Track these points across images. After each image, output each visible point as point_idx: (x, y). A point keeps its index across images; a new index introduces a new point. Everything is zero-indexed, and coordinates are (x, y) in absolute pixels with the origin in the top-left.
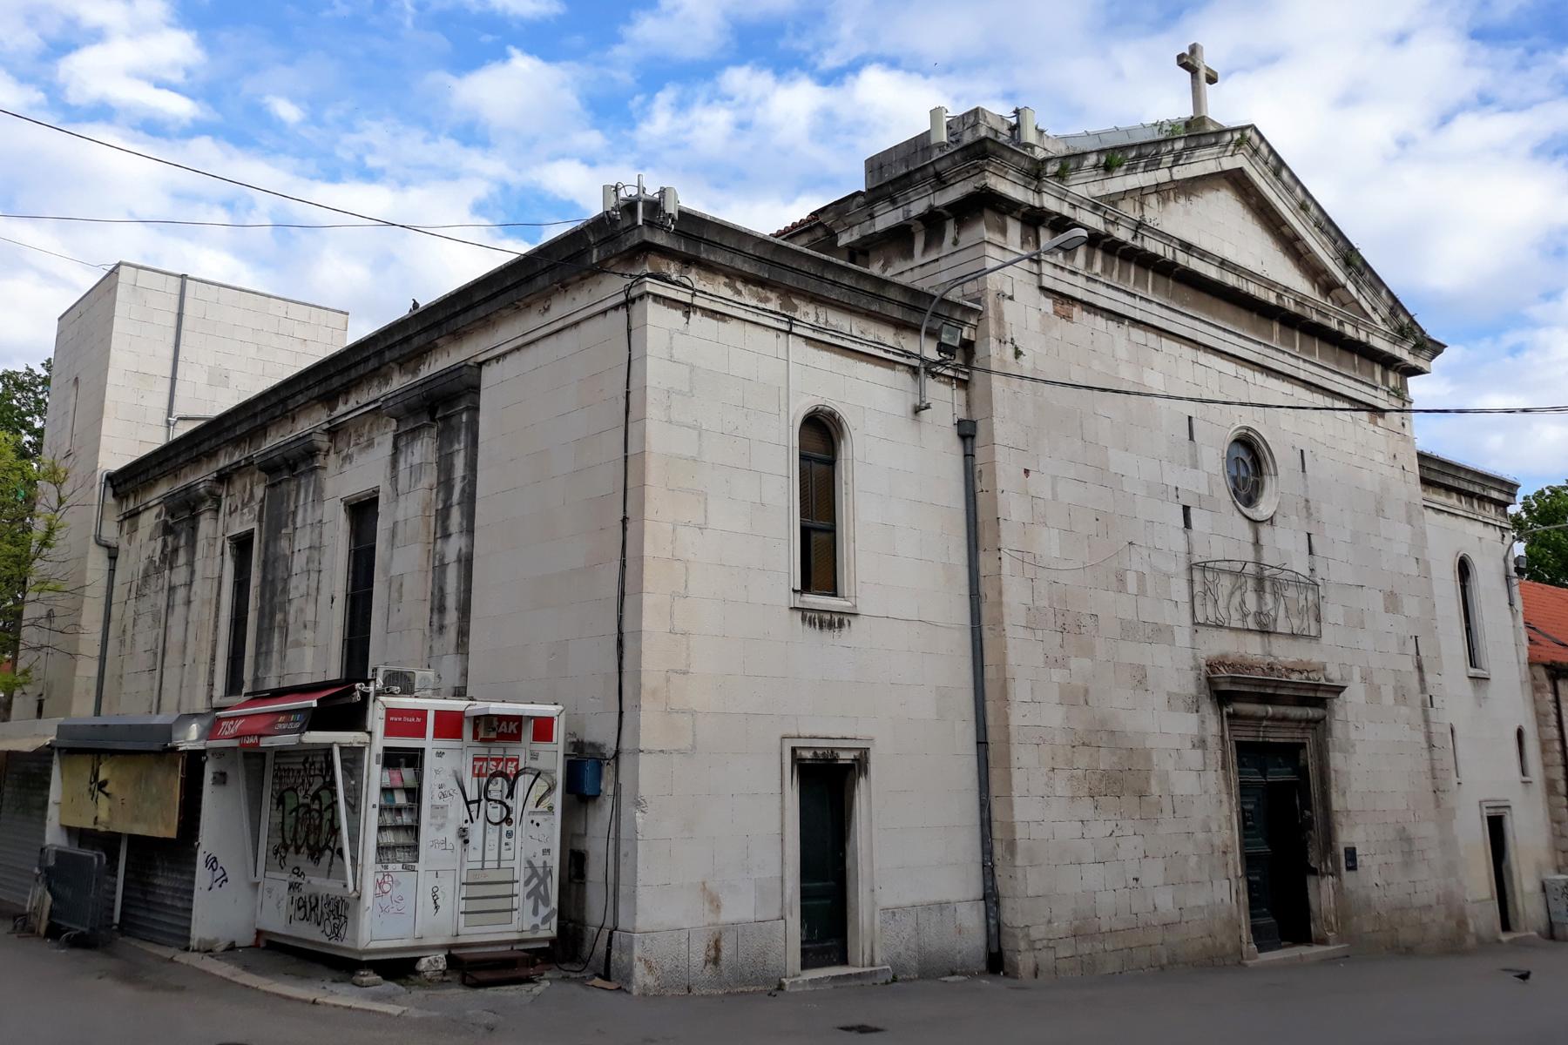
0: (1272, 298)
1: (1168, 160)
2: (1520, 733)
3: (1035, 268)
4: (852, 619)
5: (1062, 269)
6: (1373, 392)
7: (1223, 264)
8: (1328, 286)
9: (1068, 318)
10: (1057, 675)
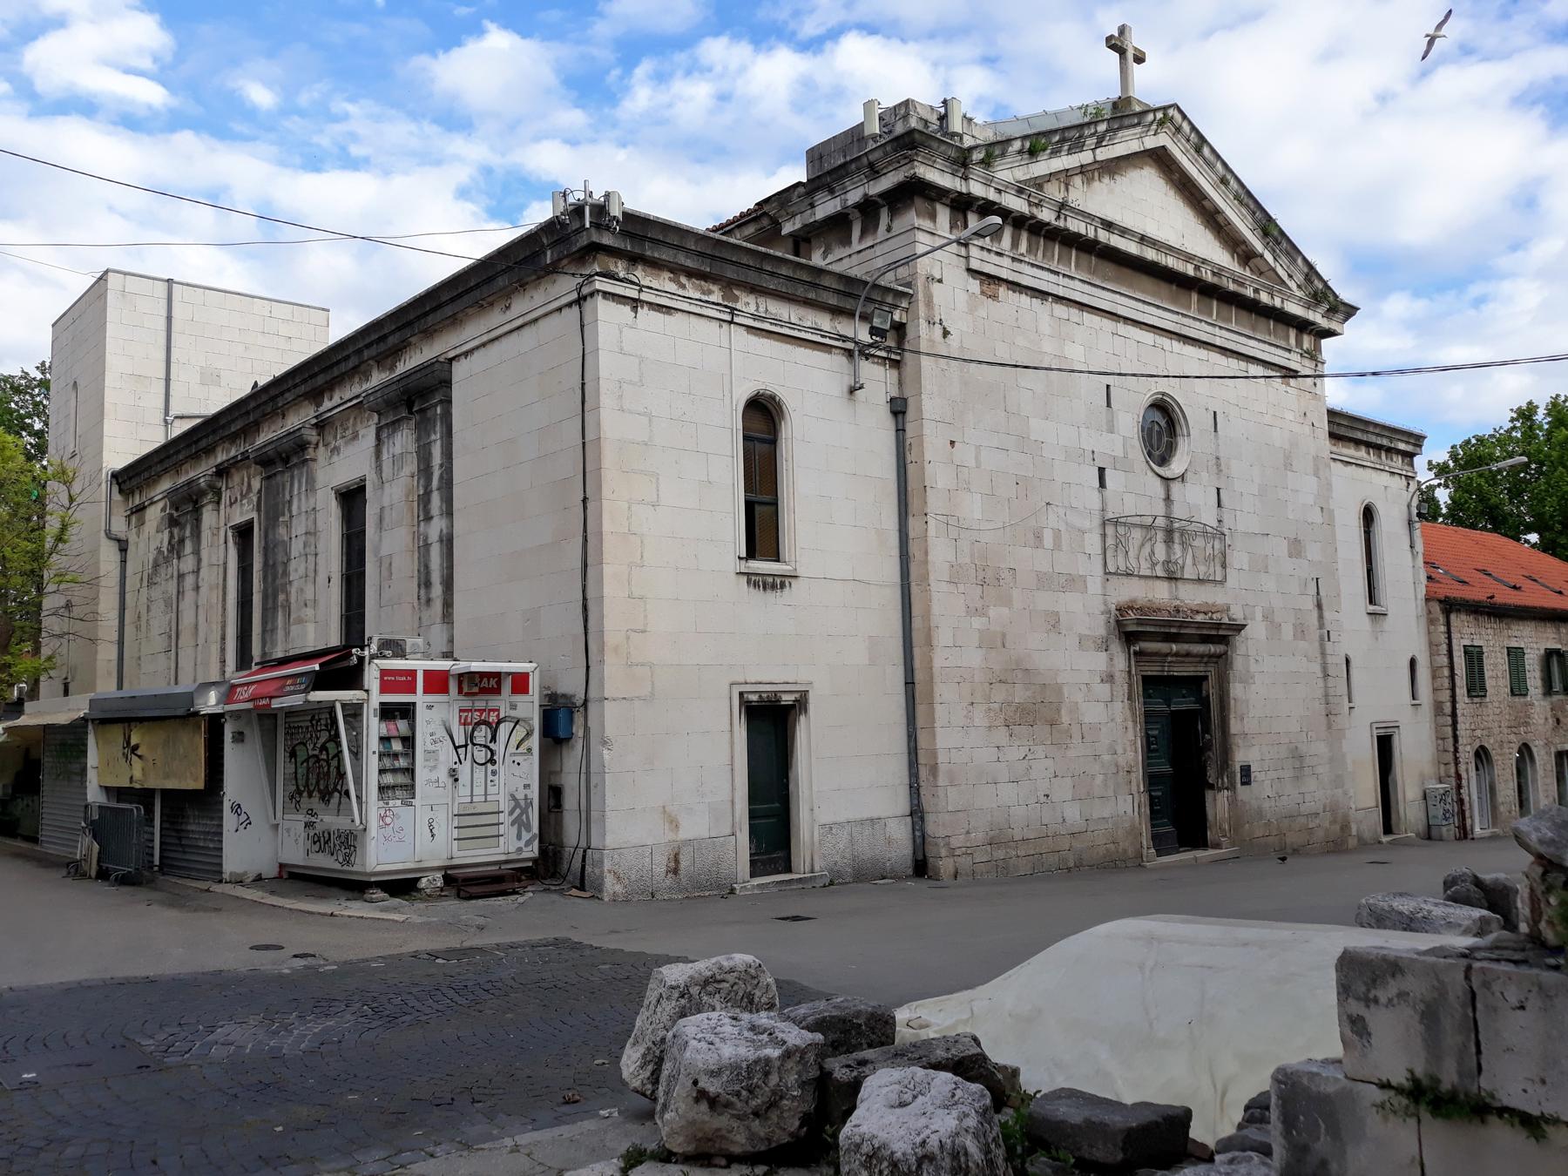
0: (1190, 271)
1: (1091, 142)
2: (1413, 662)
3: (963, 251)
4: (793, 581)
6: (1286, 355)
7: (1143, 239)
8: (1247, 257)
9: (994, 297)
10: (977, 623)
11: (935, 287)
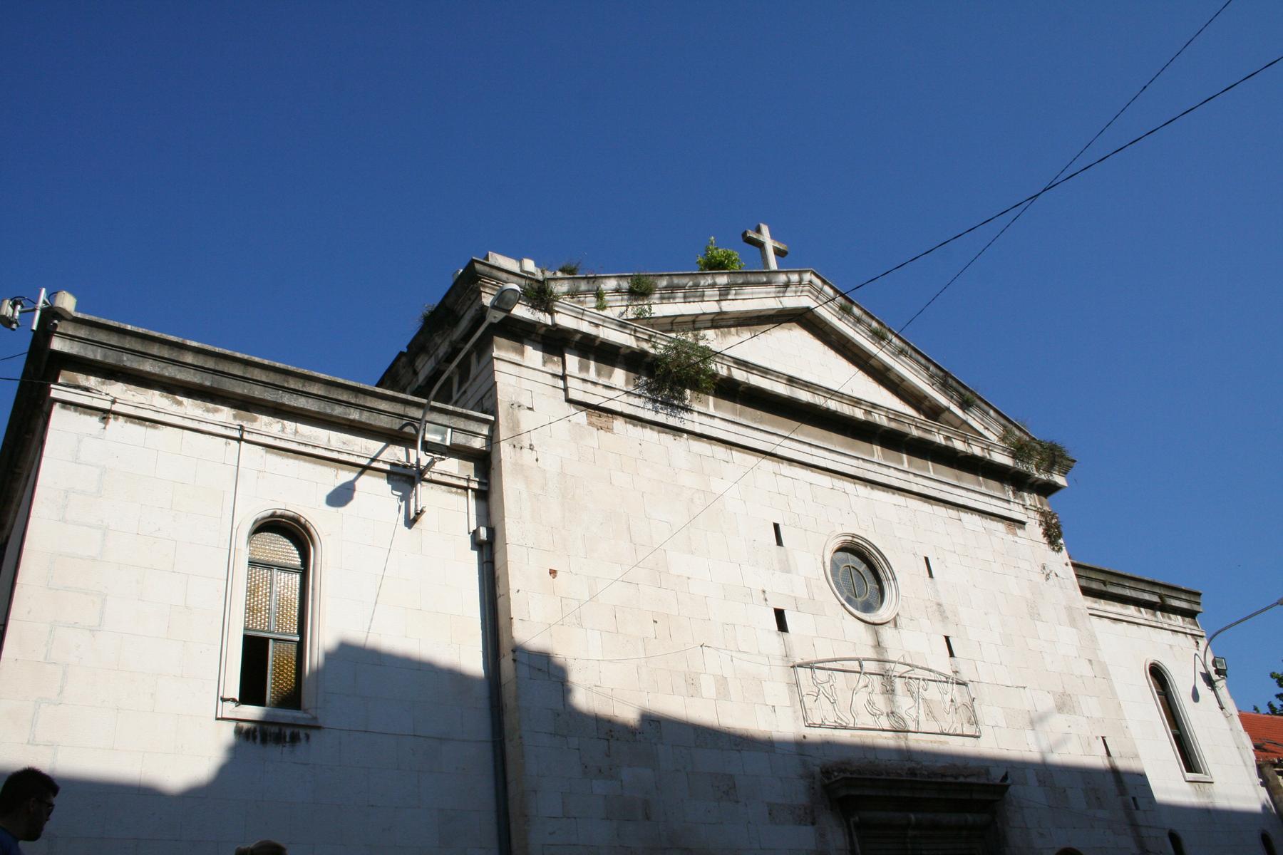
0: (859, 414)
3: (561, 383)
4: (313, 733)
5: (595, 383)
6: (1005, 505)
7: (792, 381)
8: (934, 413)
9: (609, 429)
11: (524, 416)
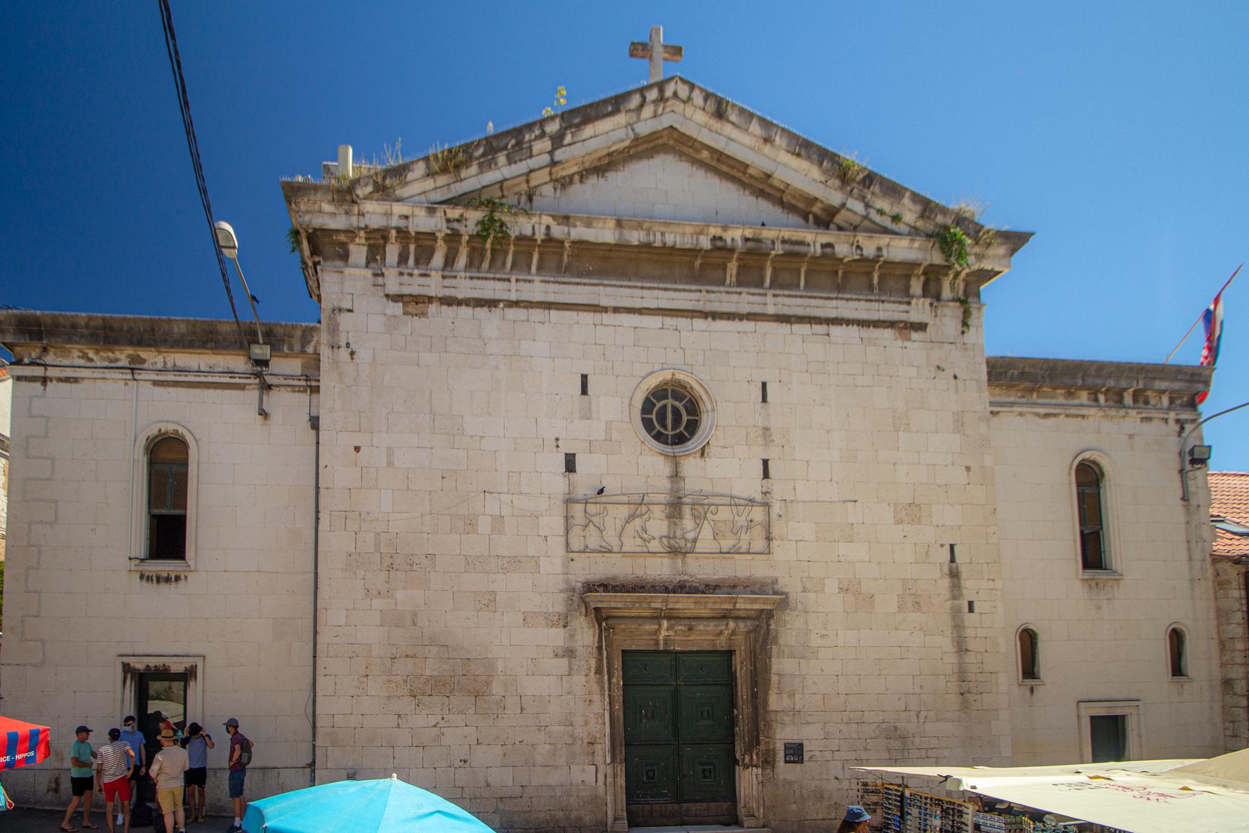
2: (1176, 638)
9: (424, 314)
10: (378, 604)
11: (344, 319)
